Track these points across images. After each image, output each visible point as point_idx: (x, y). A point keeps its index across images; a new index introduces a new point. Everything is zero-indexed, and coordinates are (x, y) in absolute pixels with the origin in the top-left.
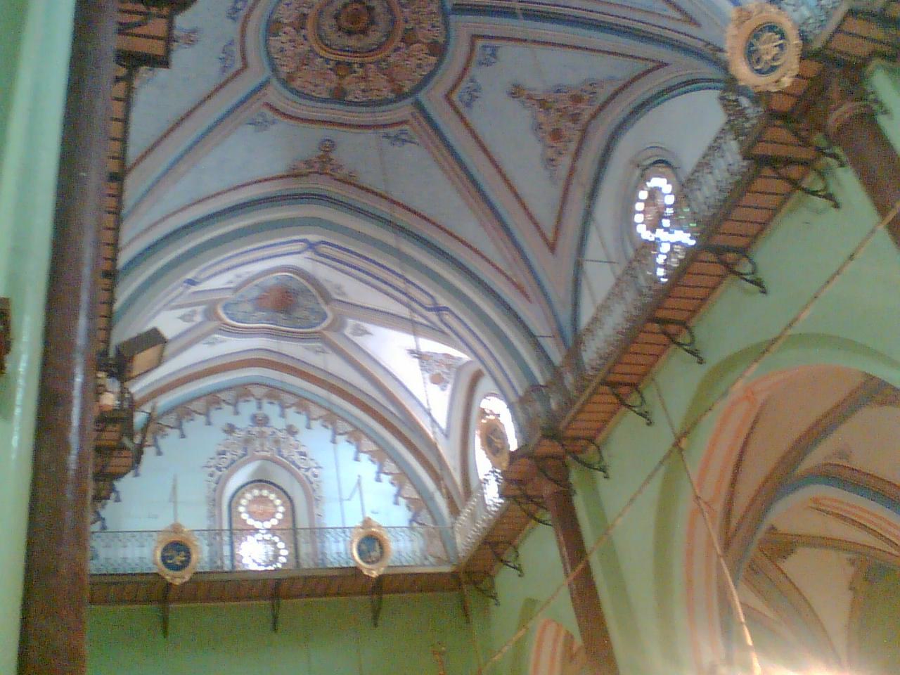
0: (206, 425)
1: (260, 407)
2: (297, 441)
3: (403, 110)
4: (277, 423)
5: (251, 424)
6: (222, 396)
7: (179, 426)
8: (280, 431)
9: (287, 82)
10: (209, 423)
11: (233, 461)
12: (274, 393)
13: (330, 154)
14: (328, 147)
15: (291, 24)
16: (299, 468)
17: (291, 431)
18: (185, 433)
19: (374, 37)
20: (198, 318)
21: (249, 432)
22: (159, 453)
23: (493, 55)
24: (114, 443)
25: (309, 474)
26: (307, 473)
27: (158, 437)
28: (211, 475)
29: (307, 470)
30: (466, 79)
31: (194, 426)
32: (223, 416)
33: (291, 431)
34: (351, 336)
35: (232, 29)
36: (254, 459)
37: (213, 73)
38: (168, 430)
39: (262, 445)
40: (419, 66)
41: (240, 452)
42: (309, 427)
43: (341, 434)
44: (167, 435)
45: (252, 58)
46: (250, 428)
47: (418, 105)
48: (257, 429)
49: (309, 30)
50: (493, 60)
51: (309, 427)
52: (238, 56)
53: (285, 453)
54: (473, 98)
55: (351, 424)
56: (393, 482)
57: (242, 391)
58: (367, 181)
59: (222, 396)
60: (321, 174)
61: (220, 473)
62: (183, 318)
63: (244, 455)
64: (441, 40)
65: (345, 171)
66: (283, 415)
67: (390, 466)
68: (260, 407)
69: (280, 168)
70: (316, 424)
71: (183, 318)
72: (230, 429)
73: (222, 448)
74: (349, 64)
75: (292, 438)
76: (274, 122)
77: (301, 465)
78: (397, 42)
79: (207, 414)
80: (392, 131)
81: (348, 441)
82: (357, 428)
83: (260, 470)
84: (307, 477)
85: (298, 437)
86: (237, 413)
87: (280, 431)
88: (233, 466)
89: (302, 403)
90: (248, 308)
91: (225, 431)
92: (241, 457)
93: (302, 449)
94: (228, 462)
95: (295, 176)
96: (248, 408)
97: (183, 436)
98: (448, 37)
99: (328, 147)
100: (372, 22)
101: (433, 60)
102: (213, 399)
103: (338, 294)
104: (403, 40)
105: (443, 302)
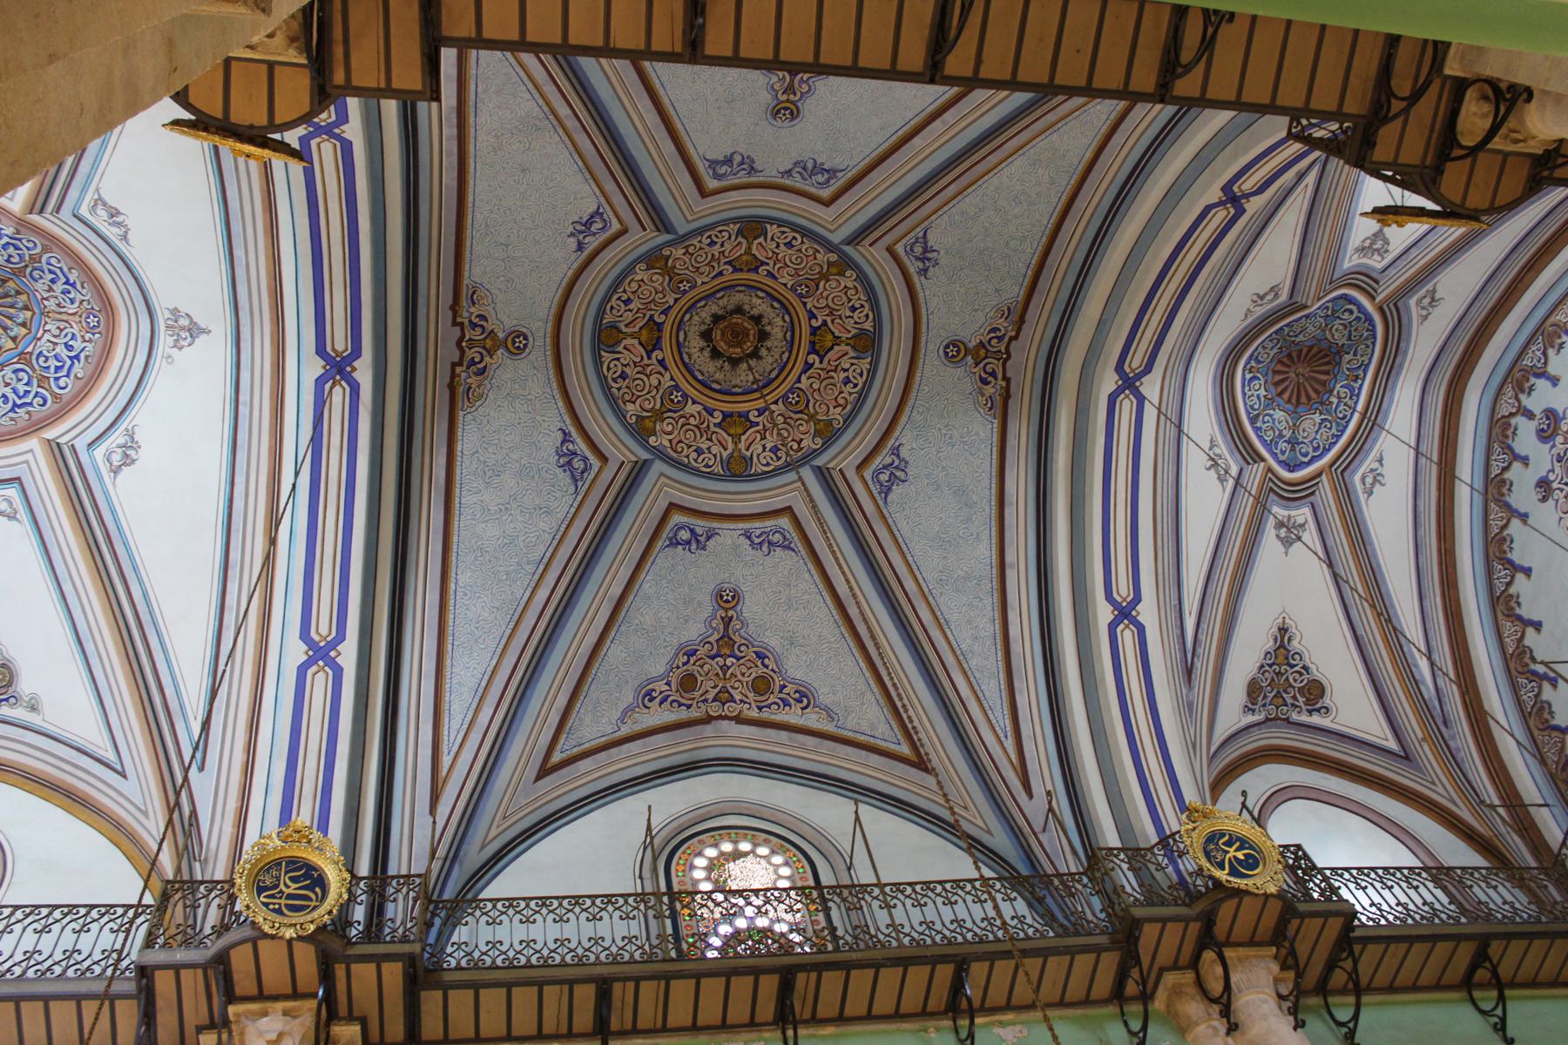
1: (1530, 415)
3: (873, 256)
5: (1548, 446)
6: (1495, 471)
7: (1515, 568)
9: (828, 434)
12: (1519, 377)
13: (971, 345)
14: (955, 351)
15: (737, 439)
19: (759, 305)
20: (1303, 514)
23: (728, 161)
24: (1194, 928)
27: (1518, 611)
30: (788, 182)
34: (1389, 258)
35: (729, 535)
37: (789, 564)
38: (1512, 590)
40: (789, 245)
44: (1518, 597)
45: (778, 502)
47: (855, 239)
49: (750, 406)
50: (738, 159)
52: (769, 523)
54: (818, 169)
57: (1499, 431)
58: (1014, 292)
59: (1495, 471)
60: (1009, 357)
62: (1287, 543)
64: (734, 228)
65: (1001, 323)
68: (1530, 415)
69: (983, 429)
71: (1287, 543)
74: (814, 331)
76: (896, 451)
78: (760, 276)
80: (913, 267)
90: (1311, 423)
91: (1544, 499)
95: (1007, 396)
96: (1525, 437)
98: (725, 222)
99: (955, 351)
100: (739, 310)
101: (772, 230)
102: (1495, 489)
103: (1276, 296)
104: (756, 270)
105: (1214, 195)
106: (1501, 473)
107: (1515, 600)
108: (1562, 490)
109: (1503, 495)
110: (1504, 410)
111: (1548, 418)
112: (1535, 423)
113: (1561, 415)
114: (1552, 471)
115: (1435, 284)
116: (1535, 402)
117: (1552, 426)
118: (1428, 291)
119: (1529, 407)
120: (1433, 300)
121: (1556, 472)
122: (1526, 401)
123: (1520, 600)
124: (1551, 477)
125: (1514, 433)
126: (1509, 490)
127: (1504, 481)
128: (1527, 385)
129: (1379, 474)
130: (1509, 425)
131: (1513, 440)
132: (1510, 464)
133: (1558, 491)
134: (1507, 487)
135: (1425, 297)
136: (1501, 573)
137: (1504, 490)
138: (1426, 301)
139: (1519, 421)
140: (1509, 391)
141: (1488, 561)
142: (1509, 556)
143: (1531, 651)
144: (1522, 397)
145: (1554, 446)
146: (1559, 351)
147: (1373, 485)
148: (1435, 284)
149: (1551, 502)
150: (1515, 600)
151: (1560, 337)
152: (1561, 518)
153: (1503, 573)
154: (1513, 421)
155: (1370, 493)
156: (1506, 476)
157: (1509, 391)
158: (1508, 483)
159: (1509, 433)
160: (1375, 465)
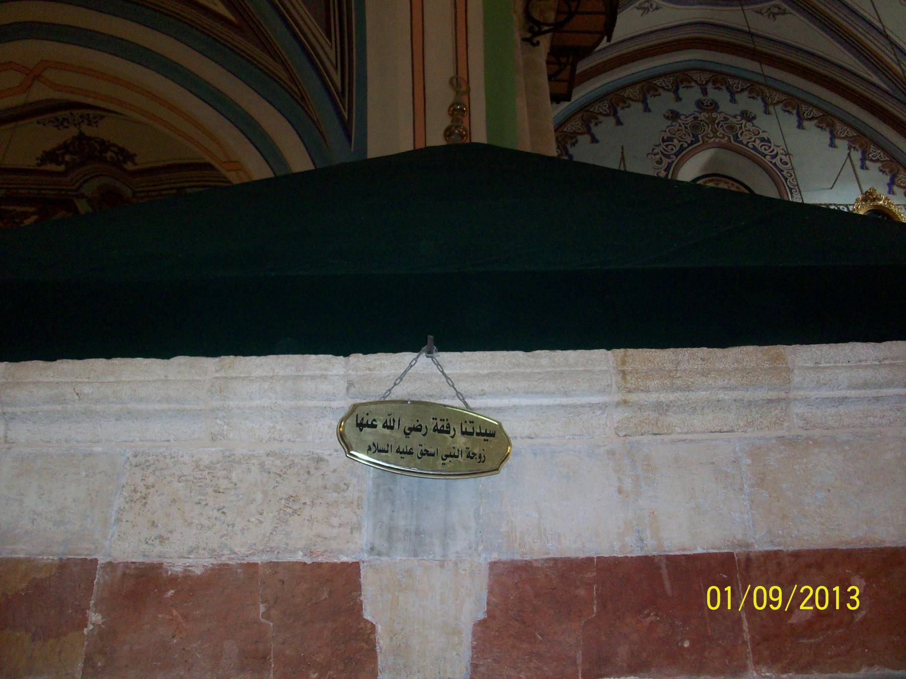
0: (645, 111)
1: (705, 92)
2: (753, 126)
4: (726, 106)
5: (697, 110)
8: (735, 117)
10: (647, 109)
11: (682, 149)
12: (719, 78)
16: (765, 156)
17: (747, 116)
18: (622, 120)
21: (696, 118)
22: (594, 140)
25: (777, 161)
26: (774, 161)
27: (592, 125)
28: (660, 162)
31: (632, 113)
32: (662, 102)
36: (705, 146)
38: (601, 118)
39: (715, 132)
41: (689, 139)
42: (767, 112)
43: (810, 119)
44: (601, 122)
46: (697, 114)
53: (744, 139)
55: (819, 109)
56: (884, 170)
63: (692, 143)
66: (733, 100)
67: (874, 153)
68: (705, 92)
72: (674, 116)
73: (667, 135)
77: (766, 152)
79: (644, 101)
81: (818, 127)
82: (826, 114)
83: (713, 161)
84: (775, 164)
86: (678, 99)
87: (735, 117)
89: (754, 88)
91: (668, 118)
92: (689, 145)
93: (762, 135)
96: (691, 95)
97: (619, 123)
106: (660, 87)
107: (597, 121)
108: (680, 126)
109: (649, 92)
110: (696, 76)
111: (711, 104)
112: (704, 98)
113: (720, 110)
114: (686, 117)
115: (790, 13)
116: (713, 94)
117: (709, 108)
118: (785, 9)
119: (709, 90)
120: (774, 15)
121: (688, 119)
122: (710, 86)
123: (599, 125)
124: (682, 117)
125: (688, 87)
126: (655, 96)
127: (657, 90)
128: (719, 85)
129: (648, 11)
130: (690, 82)
131: (684, 87)
132: (669, 90)
133: (678, 125)
134: (655, 93)
135: (780, 9)
136: (605, 107)
137: (652, 93)
138: (776, 10)
140: (707, 76)
141: (606, 95)
142: (619, 109)
143: (576, 142)
144: (710, 86)
145: (700, 113)
146: (750, 97)
147: (643, 8)
148: (790, 13)
149: (670, 122)
150: (597, 121)
151: (758, 95)
152: (665, 131)
153: (606, 108)
154: (693, 84)
155: (638, 9)
157: (707, 76)
158: (658, 93)
159: (685, 84)
160: (654, 6)
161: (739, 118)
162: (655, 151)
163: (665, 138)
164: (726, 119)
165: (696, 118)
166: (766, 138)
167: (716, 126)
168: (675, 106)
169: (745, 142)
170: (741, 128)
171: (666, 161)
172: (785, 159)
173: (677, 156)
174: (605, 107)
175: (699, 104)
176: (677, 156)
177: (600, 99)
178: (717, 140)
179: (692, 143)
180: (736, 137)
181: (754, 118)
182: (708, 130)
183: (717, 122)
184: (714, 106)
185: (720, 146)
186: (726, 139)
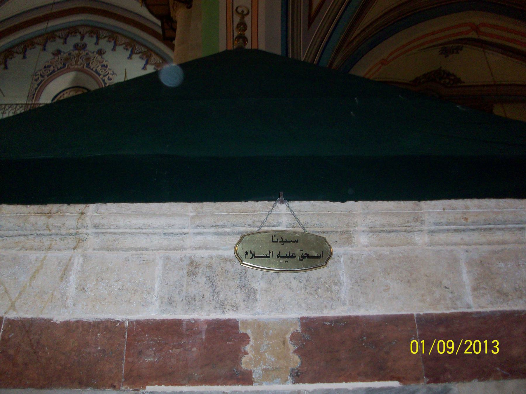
0: (43, 50)
1: (82, 38)
11: (54, 71)
16: (99, 75)
28: (36, 80)
29: (104, 76)
33: (100, 52)
36: (69, 70)
43: (136, 53)
48: (77, 52)
51: (114, 49)
57: (72, 30)
61: (43, 79)
66: (97, 43)
68: (82, 38)
70: (120, 49)
75: (99, 58)
83: (76, 79)
84: (104, 81)
85: (104, 56)
88: (53, 75)
91: (53, 54)
92: (58, 69)
93: (105, 63)
94: (49, 72)
96: (74, 40)
102: (51, 36)
111: (83, 45)
124: (62, 54)
127: (55, 38)
128: (92, 34)
136: (21, 48)
139: (79, 37)
140: (88, 29)
156: (57, 38)
161: (95, 53)
162: (37, 74)
163: (46, 66)
164: (87, 54)
165: (70, 54)
166: (106, 65)
167: (79, 58)
168: (63, 48)
169: (92, 68)
170: (94, 59)
171: (41, 79)
172: (111, 76)
173: (48, 76)
174: (21, 48)
175: (76, 47)
176: (48, 76)
177: (19, 44)
178: (76, 67)
179: (61, 68)
180: (88, 66)
181: (104, 53)
182: (74, 61)
183: (81, 56)
184: (84, 46)
185: (77, 70)
186: (82, 66)
